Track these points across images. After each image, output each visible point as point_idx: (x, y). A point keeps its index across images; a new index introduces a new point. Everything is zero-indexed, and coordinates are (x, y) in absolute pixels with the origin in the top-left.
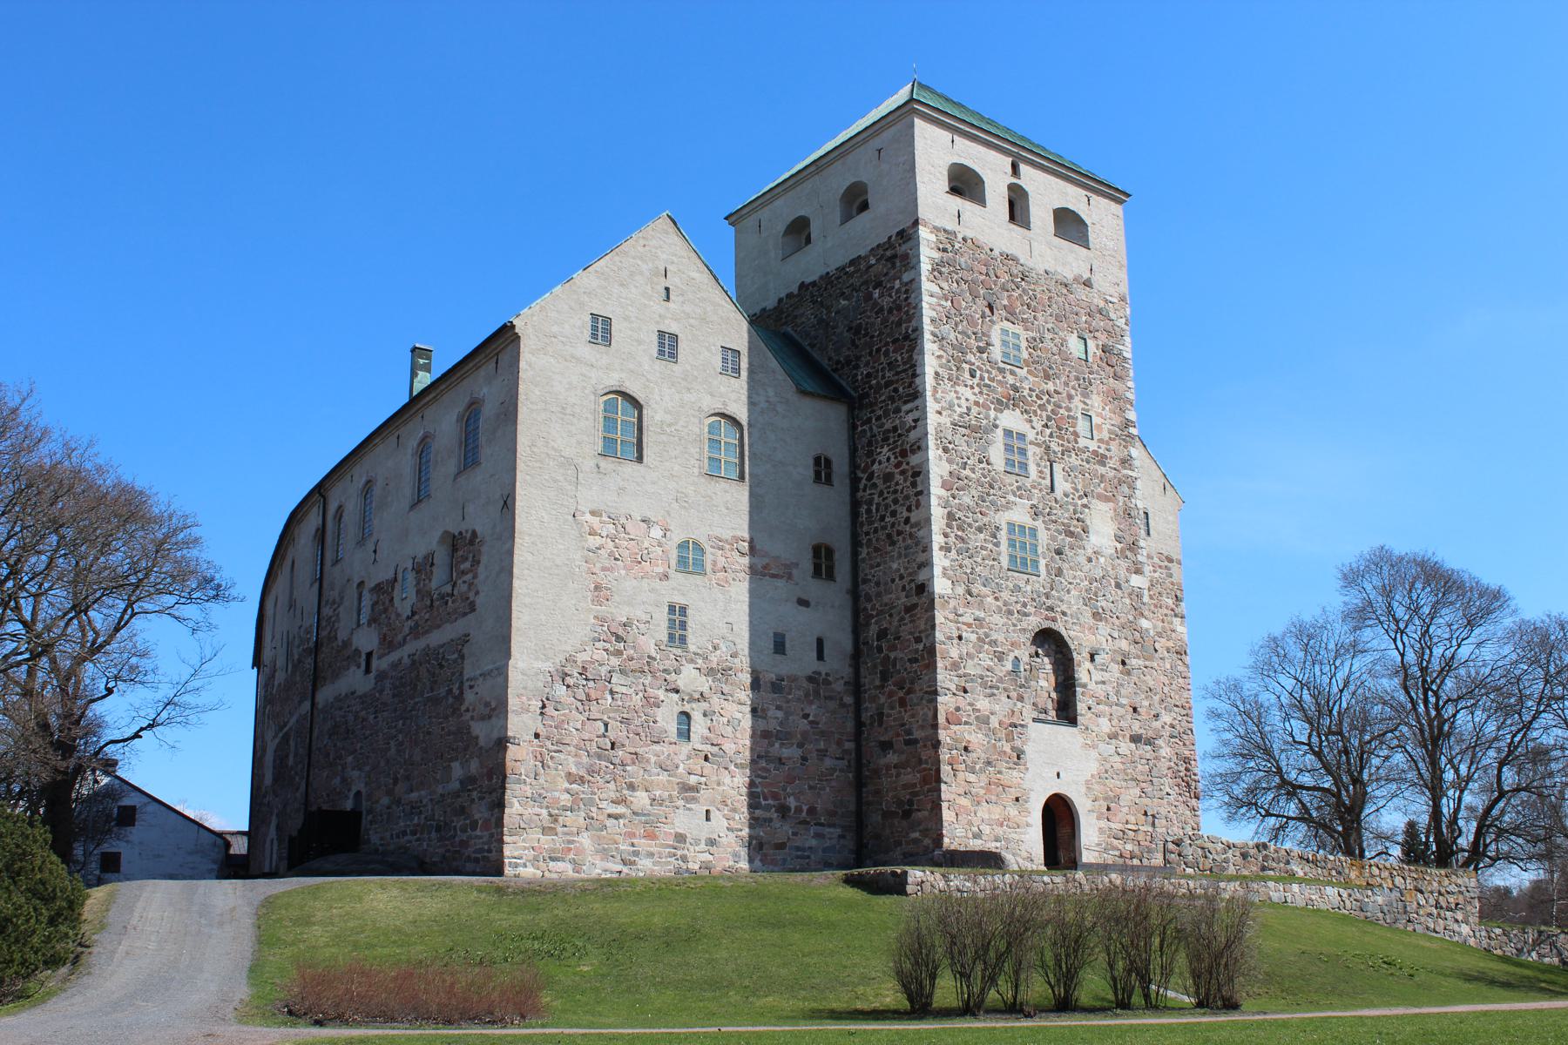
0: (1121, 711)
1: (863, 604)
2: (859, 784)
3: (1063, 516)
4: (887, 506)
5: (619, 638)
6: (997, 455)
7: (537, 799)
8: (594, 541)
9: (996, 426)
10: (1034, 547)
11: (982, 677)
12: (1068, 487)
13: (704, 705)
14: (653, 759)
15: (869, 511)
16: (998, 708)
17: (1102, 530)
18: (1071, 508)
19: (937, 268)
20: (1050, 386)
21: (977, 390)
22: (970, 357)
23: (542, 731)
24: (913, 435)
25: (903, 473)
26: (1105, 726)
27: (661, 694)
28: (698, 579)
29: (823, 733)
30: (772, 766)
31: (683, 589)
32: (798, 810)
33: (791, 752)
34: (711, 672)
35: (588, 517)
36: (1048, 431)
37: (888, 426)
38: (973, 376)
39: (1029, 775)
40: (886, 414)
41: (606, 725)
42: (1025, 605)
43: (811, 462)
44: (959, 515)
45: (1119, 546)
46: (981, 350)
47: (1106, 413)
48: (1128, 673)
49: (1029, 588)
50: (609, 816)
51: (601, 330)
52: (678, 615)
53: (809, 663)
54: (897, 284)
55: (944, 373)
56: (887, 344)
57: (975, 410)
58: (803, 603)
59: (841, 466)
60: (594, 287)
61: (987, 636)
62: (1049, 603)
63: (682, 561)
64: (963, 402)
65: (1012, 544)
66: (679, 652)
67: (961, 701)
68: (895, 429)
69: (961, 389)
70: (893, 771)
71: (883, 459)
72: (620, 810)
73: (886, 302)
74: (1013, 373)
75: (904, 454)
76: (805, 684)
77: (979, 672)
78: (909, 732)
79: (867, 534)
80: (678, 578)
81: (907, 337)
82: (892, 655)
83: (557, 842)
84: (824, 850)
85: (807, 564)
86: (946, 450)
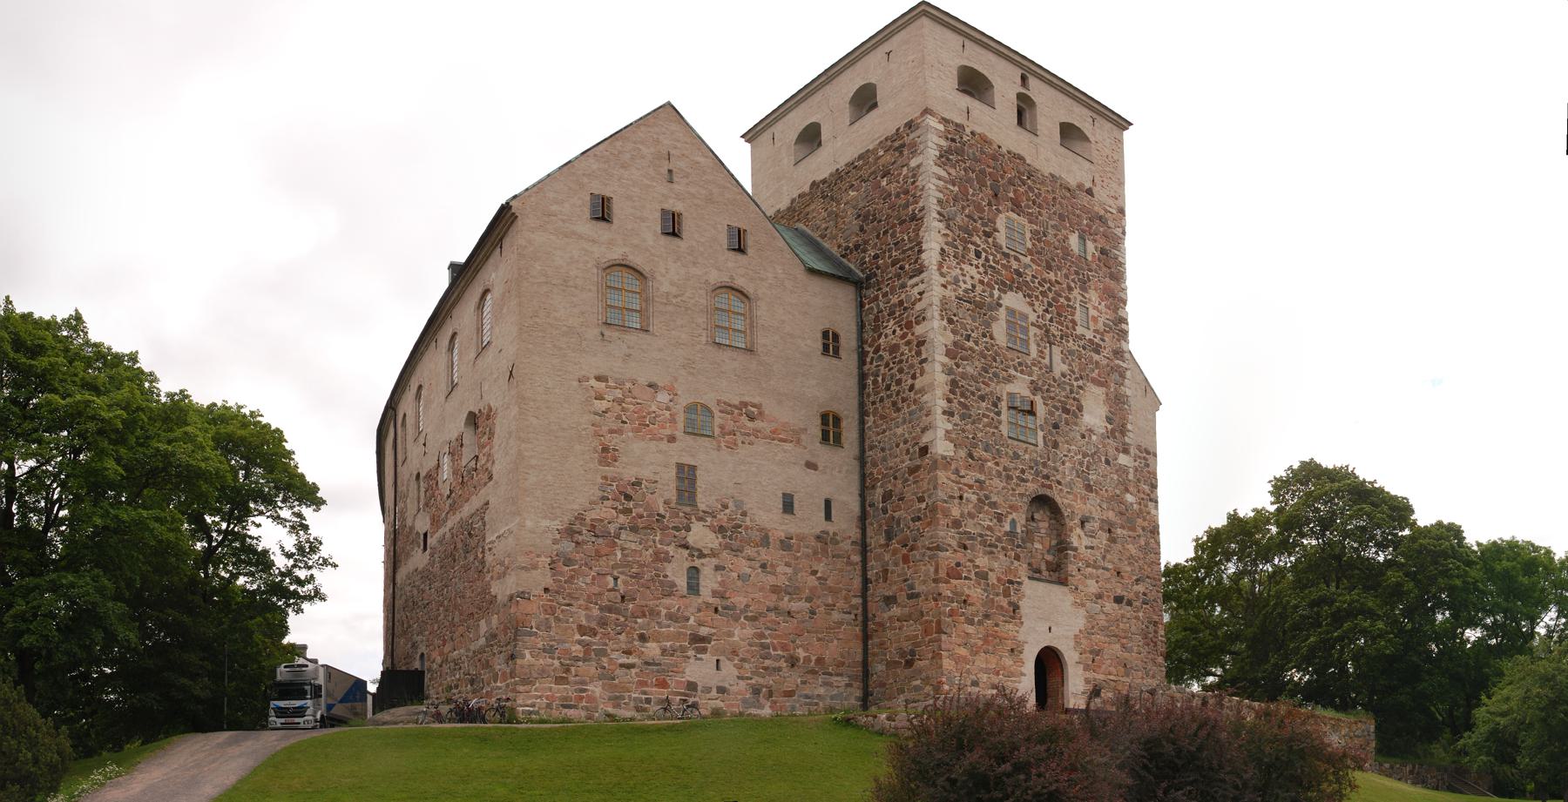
1: (869, 469)
2: (866, 637)
4: (892, 376)
5: (628, 498)
7: (549, 650)
11: (981, 535)
13: (714, 561)
14: (664, 612)
15: (875, 382)
16: (995, 565)
23: (553, 587)
24: (918, 307)
25: (908, 343)
29: (831, 590)
32: (807, 660)
34: (721, 530)
37: (895, 300)
38: (978, 255)
39: (1023, 629)
40: (893, 290)
41: (616, 579)
42: (1023, 471)
43: (819, 335)
44: (963, 383)
50: (622, 666)
53: (817, 523)
54: (905, 170)
56: (894, 226)
58: (811, 466)
59: (848, 341)
64: (967, 279)
66: (688, 509)
67: (960, 556)
68: (901, 303)
70: (897, 624)
71: (889, 331)
72: (631, 660)
73: (893, 188)
75: (909, 325)
78: (912, 587)
79: (874, 403)
80: (685, 441)
81: (914, 218)
82: (896, 515)
83: (567, 690)
84: (832, 698)
85: (816, 430)
86: (950, 321)
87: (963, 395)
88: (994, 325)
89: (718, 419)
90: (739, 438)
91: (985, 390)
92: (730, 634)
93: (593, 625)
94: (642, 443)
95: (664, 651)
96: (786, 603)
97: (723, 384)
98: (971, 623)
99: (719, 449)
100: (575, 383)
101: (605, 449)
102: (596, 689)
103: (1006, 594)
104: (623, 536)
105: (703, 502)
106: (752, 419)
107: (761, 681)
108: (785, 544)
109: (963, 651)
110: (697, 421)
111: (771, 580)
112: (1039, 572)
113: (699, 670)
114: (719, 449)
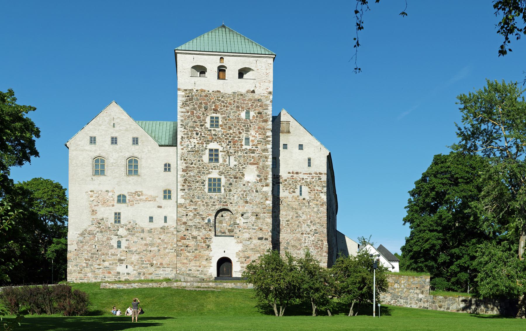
0: (255, 231)
3: (233, 173)
6: (206, 158)
7: (77, 265)
9: (206, 149)
10: (219, 185)
12: (236, 163)
13: (126, 238)
14: (110, 253)
17: (251, 175)
18: (237, 170)
19: (184, 104)
20: (231, 131)
21: (198, 139)
22: (197, 129)
26: (247, 236)
27: (112, 236)
28: (124, 205)
29: (165, 243)
32: (157, 264)
35: (89, 193)
36: (229, 147)
42: (214, 202)
43: (163, 166)
45: (258, 179)
46: (202, 126)
47: (257, 135)
48: (259, 219)
49: (216, 197)
52: (118, 216)
53: (162, 223)
57: (197, 146)
61: (198, 213)
62: (225, 200)
63: (119, 201)
65: (210, 185)
66: (118, 225)
67: (186, 233)
69: (192, 140)
72: (100, 267)
74: (214, 130)
76: (160, 230)
77: (194, 224)
84: (166, 274)
86: (185, 160)
87: (189, 183)
89: (128, 198)
91: (198, 179)
92: (131, 258)
93: (89, 258)
94: (104, 208)
95: (110, 264)
96: (149, 248)
97: (129, 185)
98: (189, 252)
99: (128, 206)
100: (84, 194)
101: (93, 211)
102: (90, 275)
103: (205, 242)
104: (98, 234)
105: (123, 222)
106: (139, 196)
107: (141, 271)
108: (150, 231)
109: (185, 261)
110: (122, 199)
111: (144, 242)
113: (122, 268)
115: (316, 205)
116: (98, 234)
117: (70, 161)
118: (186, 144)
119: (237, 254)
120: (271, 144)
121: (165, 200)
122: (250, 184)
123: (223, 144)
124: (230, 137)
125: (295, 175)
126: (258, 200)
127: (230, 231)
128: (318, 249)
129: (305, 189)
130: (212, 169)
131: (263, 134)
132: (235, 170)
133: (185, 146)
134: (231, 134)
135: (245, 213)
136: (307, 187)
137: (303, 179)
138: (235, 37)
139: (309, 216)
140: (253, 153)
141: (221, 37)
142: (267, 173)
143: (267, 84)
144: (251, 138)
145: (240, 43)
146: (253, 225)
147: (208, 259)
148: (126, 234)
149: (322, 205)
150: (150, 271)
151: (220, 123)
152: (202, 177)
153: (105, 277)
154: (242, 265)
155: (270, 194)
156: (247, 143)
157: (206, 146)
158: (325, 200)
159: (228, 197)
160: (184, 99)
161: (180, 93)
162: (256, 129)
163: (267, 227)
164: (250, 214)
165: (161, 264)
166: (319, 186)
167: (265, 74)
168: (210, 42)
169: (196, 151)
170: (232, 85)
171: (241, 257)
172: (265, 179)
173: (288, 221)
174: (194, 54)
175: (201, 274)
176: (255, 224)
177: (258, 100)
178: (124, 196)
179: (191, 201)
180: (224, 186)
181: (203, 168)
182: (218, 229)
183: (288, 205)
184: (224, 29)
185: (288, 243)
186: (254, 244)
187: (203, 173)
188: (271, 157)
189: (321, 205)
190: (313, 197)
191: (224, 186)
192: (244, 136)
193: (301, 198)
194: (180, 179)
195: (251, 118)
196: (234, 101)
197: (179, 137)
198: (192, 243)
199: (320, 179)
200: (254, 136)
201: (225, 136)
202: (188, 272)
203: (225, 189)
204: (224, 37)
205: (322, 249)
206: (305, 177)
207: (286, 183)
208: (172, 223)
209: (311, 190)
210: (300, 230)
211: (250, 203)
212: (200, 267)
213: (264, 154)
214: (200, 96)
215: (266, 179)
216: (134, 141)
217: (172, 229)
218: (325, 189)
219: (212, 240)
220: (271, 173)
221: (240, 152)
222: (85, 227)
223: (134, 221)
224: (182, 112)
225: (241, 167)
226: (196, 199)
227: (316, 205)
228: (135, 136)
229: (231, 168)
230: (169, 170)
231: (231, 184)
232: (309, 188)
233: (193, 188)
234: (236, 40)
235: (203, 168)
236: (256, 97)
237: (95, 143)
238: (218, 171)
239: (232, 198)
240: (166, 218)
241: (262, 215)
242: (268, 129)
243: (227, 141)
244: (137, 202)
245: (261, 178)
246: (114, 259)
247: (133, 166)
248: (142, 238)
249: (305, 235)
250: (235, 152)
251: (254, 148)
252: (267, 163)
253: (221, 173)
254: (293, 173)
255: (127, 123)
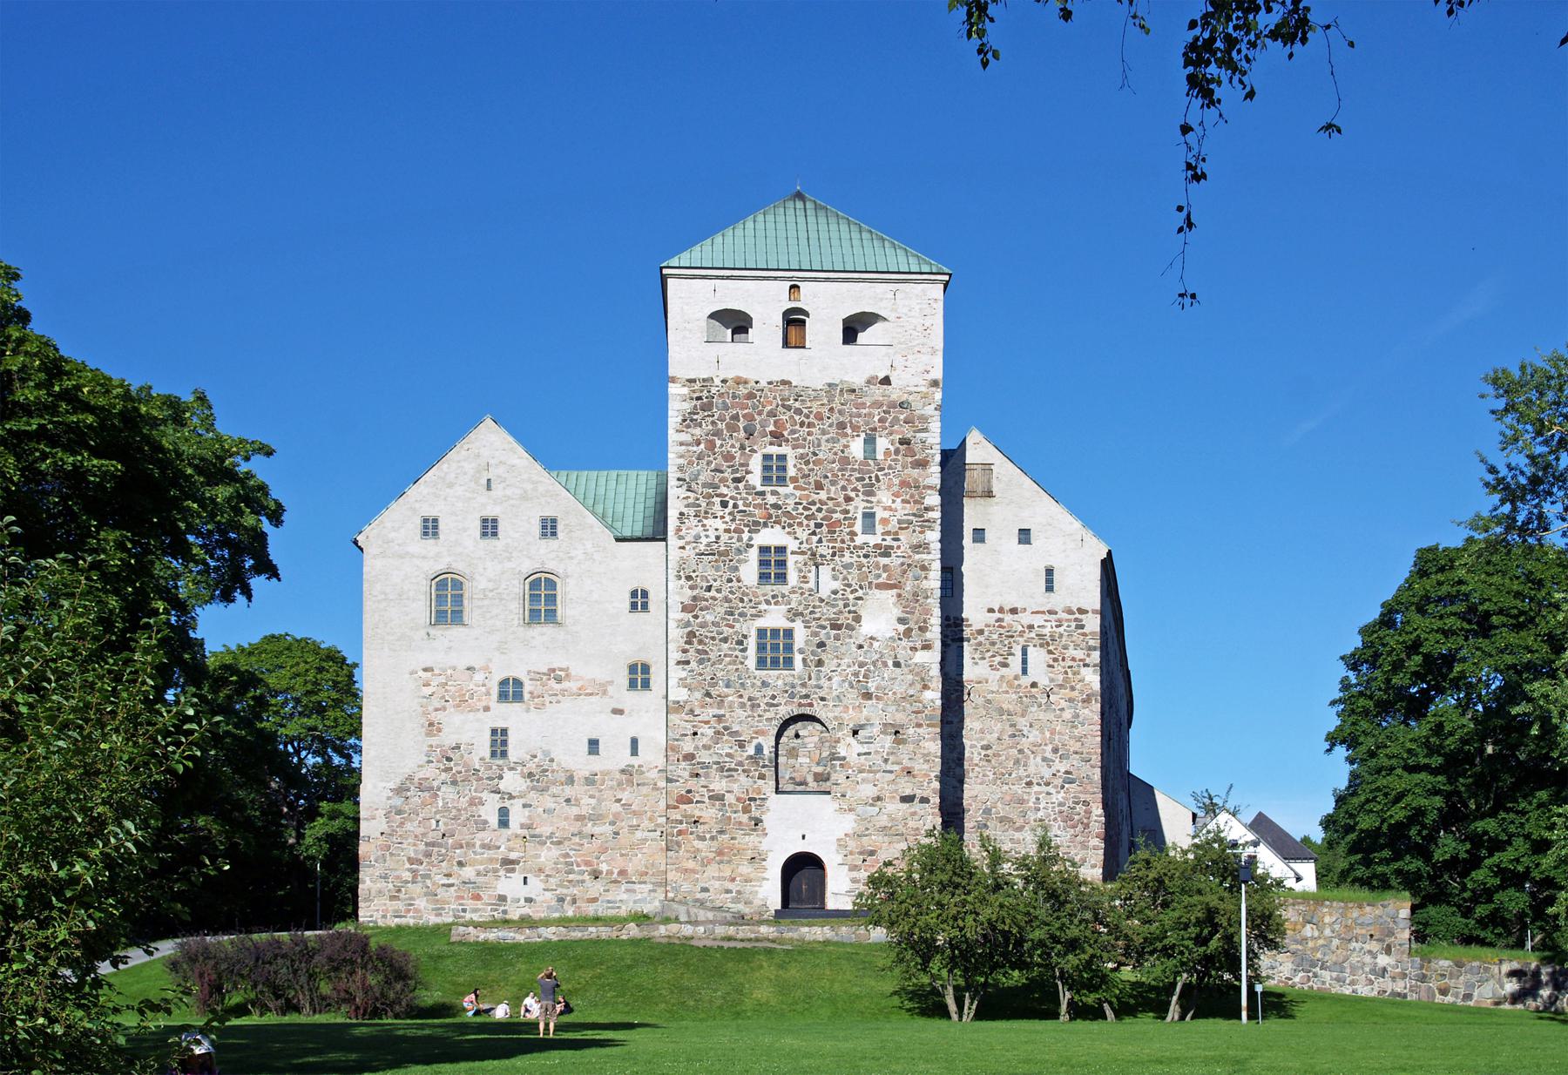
0: (892, 776)
3: (830, 612)
6: (749, 571)
7: (385, 877)
8: (427, 691)
12: (837, 585)
13: (522, 801)
16: (741, 784)
17: (879, 618)
18: (841, 603)
19: (688, 421)
20: (823, 495)
21: (728, 518)
22: (724, 490)
23: (387, 831)
26: (868, 791)
27: (485, 795)
30: (585, 841)
31: (508, 715)
32: (610, 873)
33: (605, 829)
35: (421, 673)
36: (815, 538)
42: (773, 697)
45: (901, 628)
47: (898, 504)
48: (903, 742)
49: (780, 682)
51: (430, 528)
52: (500, 738)
53: (625, 758)
55: (692, 511)
57: (725, 537)
60: (422, 497)
61: (726, 728)
62: (804, 691)
63: (503, 696)
65: (761, 648)
66: (500, 762)
72: (451, 881)
74: (774, 493)
76: (618, 776)
86: (689, 578)
87: (701, 642)
88: (742, 568)
89: (527, 688)
90: (547, 699)
91: (727, 631)
95: (478, 874)
96: (589, 828)
97: (531, 652)
98: (703, 839)
99: (528, 710)
101: (431, 724)
102: (421, 903)
103: (746, 810)
104: (443, 788)
105: (513, 754)
106: (559, 680)
107: (565, 891)
108: (590, 781)
109: (691, 864)
110: (511, 691)
111: (575, 811)
112: (804, 783)
113: (510, 885)
114: (528, 710)
115: (1071, 700)
116: (443, 788)
117: (365, 586)
118: (693, 532)
119: (841, 844)
120: (938, 528)
121: (632, 693)
122: (876, 644)
123: (799, 530)
124: (820, 510)
125: (1008, 618)
126: (900, 689)
127: (820, 778)
128: (1074, 827)
129: (1037, 656)
130: (768, 602)
131: (916, 502)
132: (834, 606)
133: (688, 539)
134: (821, 502)
135: (862, 727)
136: (1043, 651)
137: (1031, 627)
138: (833, 227)
139: (1048, 734)
140: (886, 554)
141: (791, 226)
142: (928, 612)
143: (925, 358)
144: (880, 514)
145: (846, 244)
146: (886, 761)
147: (757, 859)
148: (524, 787)
149: (1087, 701)
150: (592, 894)
151: (791, 472)
152: (737, 625)
153: (464, 911)
154: (855, 874)
155: (935, 671)
156: (869, 528)
157: (751, 539)
158: (1097, 686)
159: (813, 682)
160: (688, 406)
161: (673, 389)
162: (896, 489)
163: (926, 766)
164: (876, 730)
165: (622, 873)
166: (1076, 646)
167: (920, 328)
168: (761, 241)
169: (720, 554)
170: (824, 362)
171: (851, 853)
172: (920, 629)
173: (987, 747)
174: (717, 277)
175: (736, 900)
176: (892, 758)
177: (901, 405)
178: (518, 683)
179: (708, 694)
180: (801, 651)
181: (742, 600)
182: (785, 774)
183: (989, 702)
184: (799, 204)
185: (987, 811)
186: (889, 816)
187: (741, 615)
188: (937, 565)
189: (1084, 701)
190: (1061, 677)
191: (801, 651)
192: (858, 506)
193: (1025, 681)
194: (677, 634)
195: (880, 456)
196: (831, 410)
197: (672, 515)
198: (709, 813)
199: (1082, 627)
200: (890, 509)
201: (805, 508)
202: (699, 896)
203: (804, 660)
204: (802, 226)
205: (1087, 826)
206: (1038, 620)
207: (981, 638)
208: (652, 756)
209: (1055, 660)
210: (1022, 772)
211: (878, 698)
212: (733, 880)
213: (917, 557)
214: (734, 397)
215: (923, 629)
216: (544, 527)
217: (653, 774)
218: (1096, 656)
219: (768, 804)
220: (937, 612)
221: (847, 554)
222: (408, 771)
223: (546, 753)
224: (682, 444)
225: (851, 597)
226: (721, 689)
227: (1071, 700)
228: (549, 513)
229: (822, 600)
230: (645, 607)
231: (821, 645)
232: (1050, 652)
233: (712, 656)
234: (835, 235)
235: (742, 600)
236: (894, 397)
237: (435, 534)
238: (784, 608)
239: (823, 682)
240: (634, 742)
241: (911, 731)
242: (930, 488)
243: (812, 523)
244: (554, 699)
245: (909, 628)
246: (491, 860)
247: (542, 598)
248: (568, 801)
249: (1036, 788)
250: (834, 554)
251: (889, 542)
252: (925, 584)
253: (794, 615)
254: (1001, 610)
255: (525, 476)
